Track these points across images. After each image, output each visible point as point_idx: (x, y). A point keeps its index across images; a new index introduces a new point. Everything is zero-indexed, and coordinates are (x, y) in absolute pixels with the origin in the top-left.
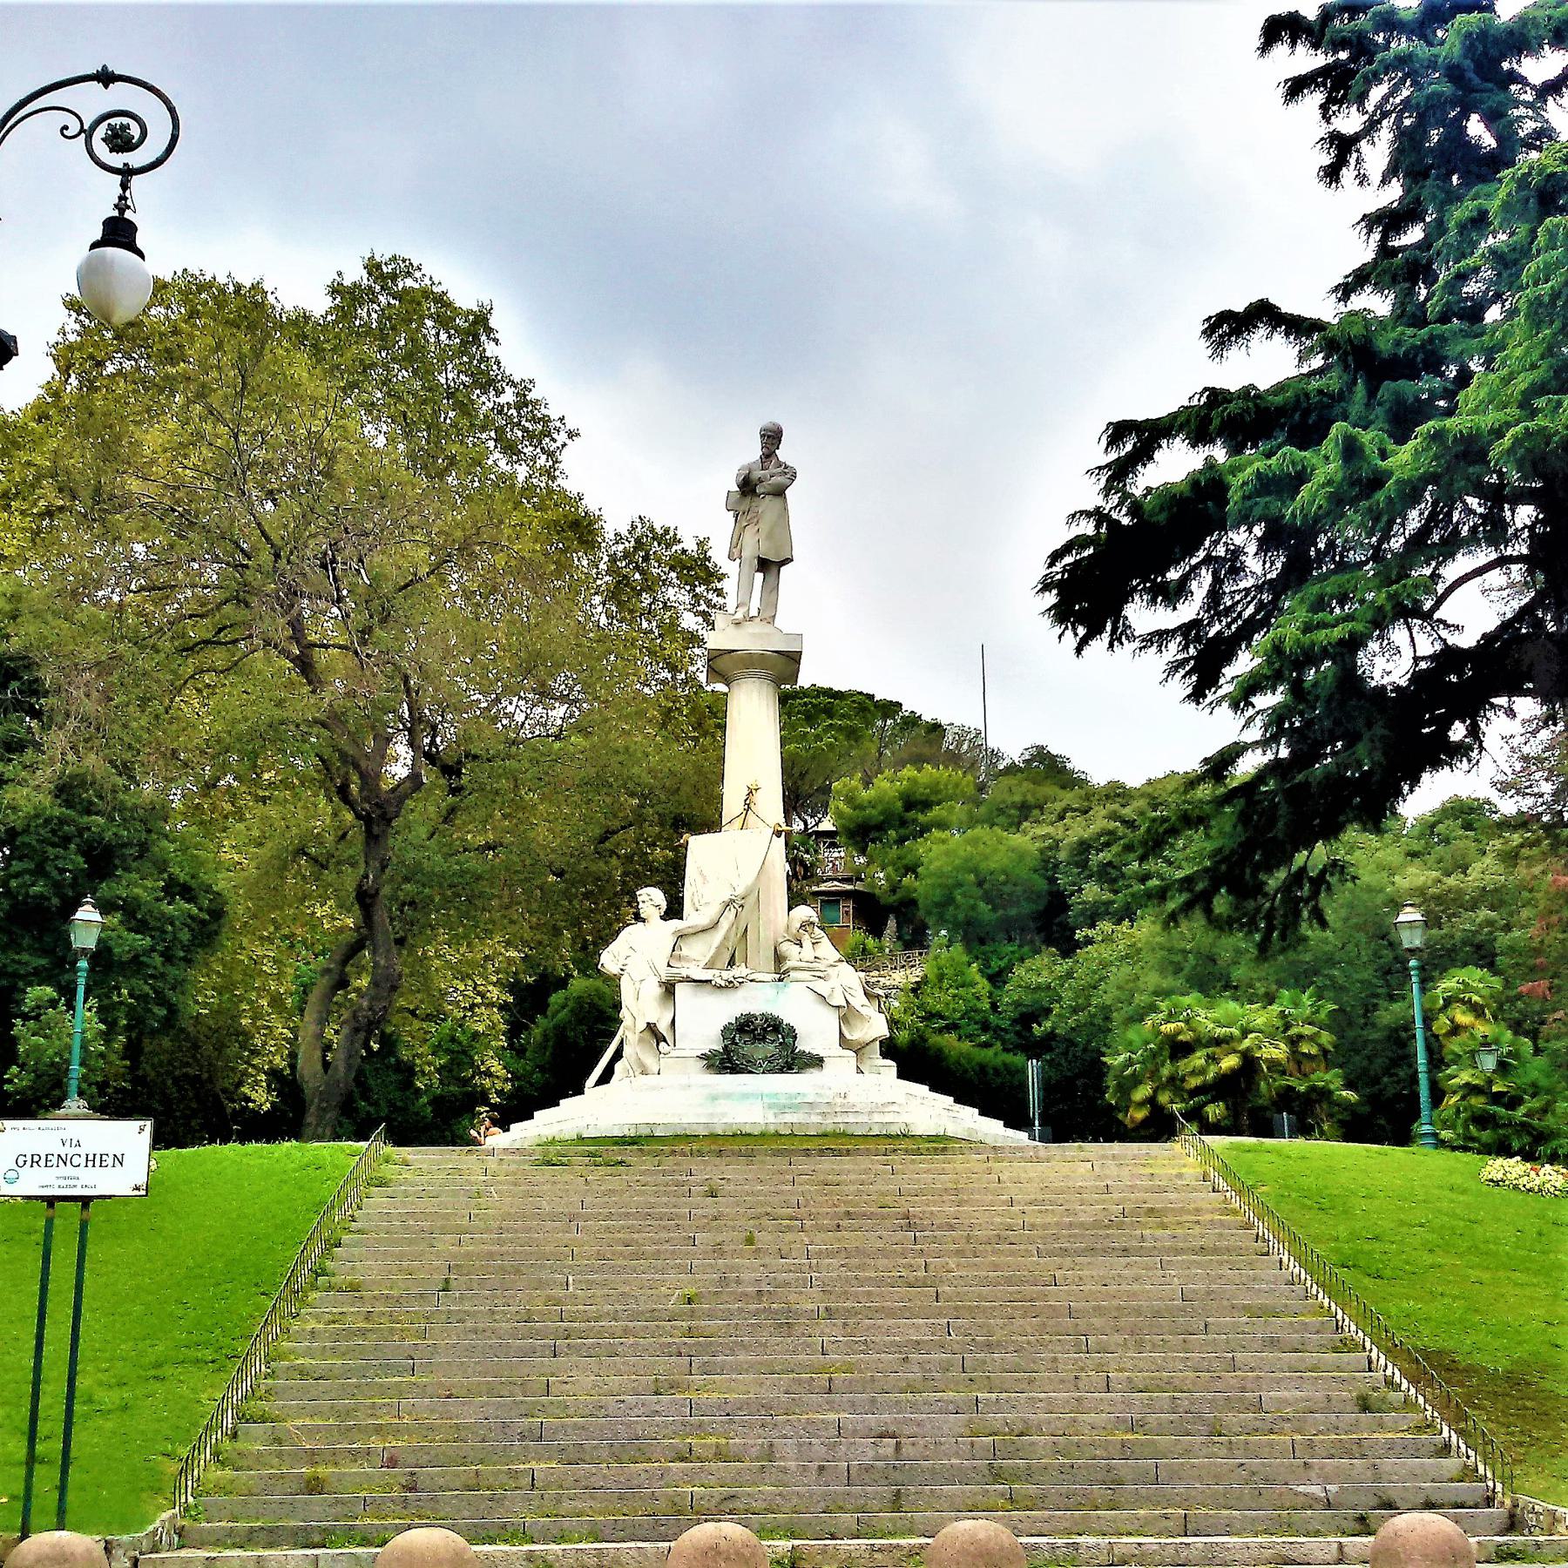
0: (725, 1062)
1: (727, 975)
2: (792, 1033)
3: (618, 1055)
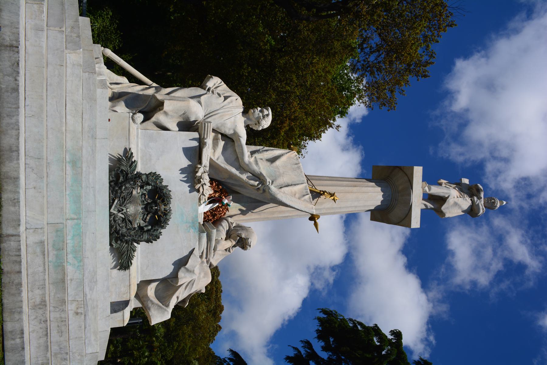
1: (206, 179)
2: (152, 237)
3: (132, 79)
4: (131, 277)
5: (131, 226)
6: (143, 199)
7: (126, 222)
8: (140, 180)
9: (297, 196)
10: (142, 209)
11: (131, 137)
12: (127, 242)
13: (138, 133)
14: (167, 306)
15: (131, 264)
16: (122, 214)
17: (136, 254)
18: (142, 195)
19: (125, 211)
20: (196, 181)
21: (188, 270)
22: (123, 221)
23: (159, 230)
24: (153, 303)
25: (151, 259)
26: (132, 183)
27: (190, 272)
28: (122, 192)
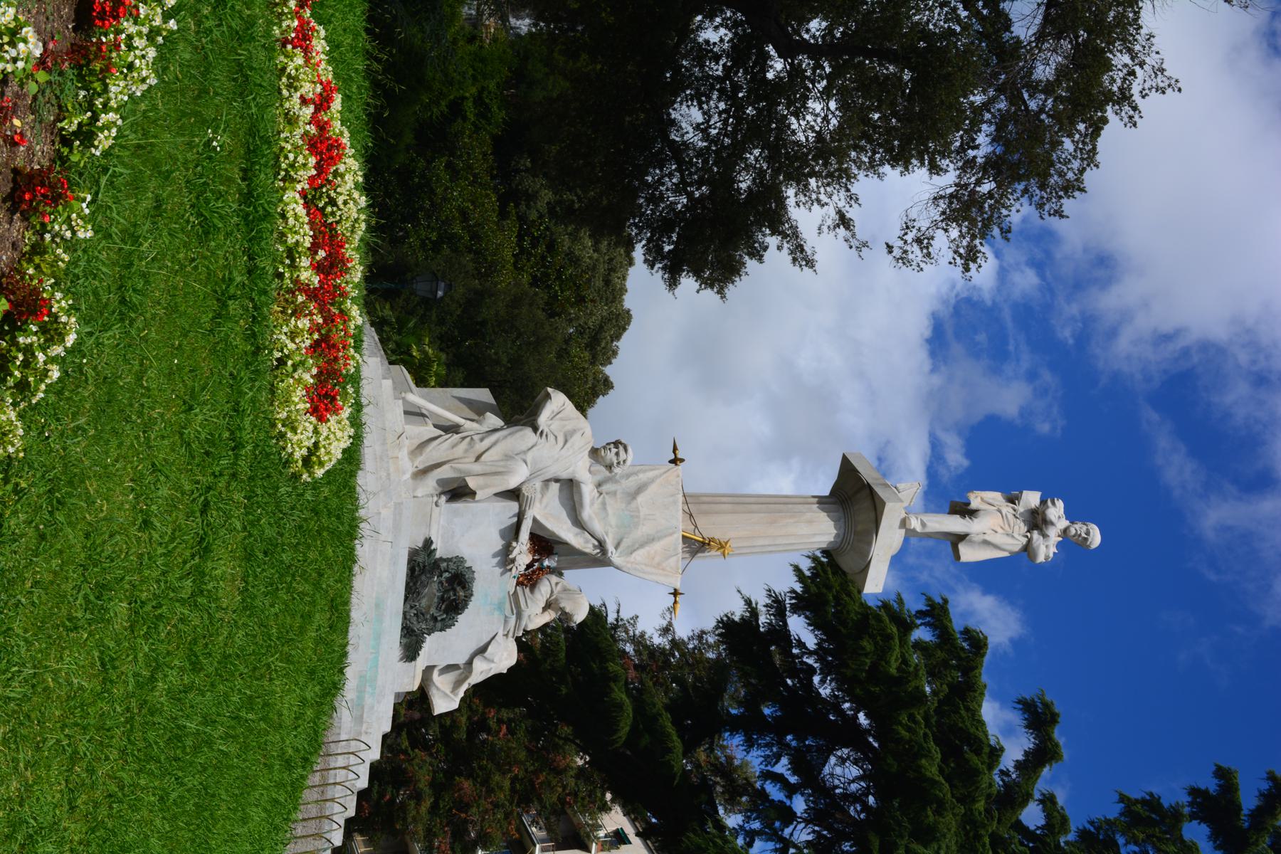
0: (423, 565)
2: (446, 625)
9: (657, 559)
14: (456, 695)
24: (438, 689)
25: (441, 647)
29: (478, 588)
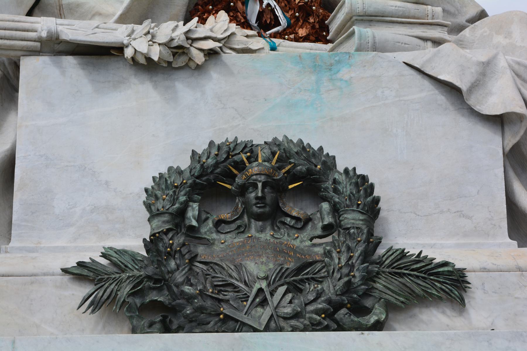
2: (365, 197)
4: (490, 266)
5: (319, 266)
6: (233, 226)
7: (302, 281)
8: (166, 239)
10: (262, 230)
11: (29, 268)
12: (370, 278)
13: (20, 249)
15: (445, 264)
16: (272, 294)
17: (413, 251)
18: (218, 232)
19: (264, 285)
20: (181, 61)
21: (474, 86)
22: (301, 291)
23: (336, 176)
26: (172, 264)
27: (483, 74)
28: (202, 293)
29: (258, 129)
